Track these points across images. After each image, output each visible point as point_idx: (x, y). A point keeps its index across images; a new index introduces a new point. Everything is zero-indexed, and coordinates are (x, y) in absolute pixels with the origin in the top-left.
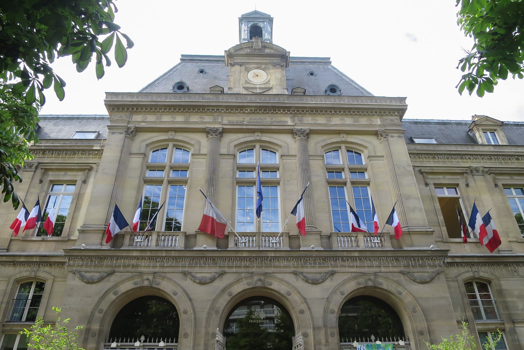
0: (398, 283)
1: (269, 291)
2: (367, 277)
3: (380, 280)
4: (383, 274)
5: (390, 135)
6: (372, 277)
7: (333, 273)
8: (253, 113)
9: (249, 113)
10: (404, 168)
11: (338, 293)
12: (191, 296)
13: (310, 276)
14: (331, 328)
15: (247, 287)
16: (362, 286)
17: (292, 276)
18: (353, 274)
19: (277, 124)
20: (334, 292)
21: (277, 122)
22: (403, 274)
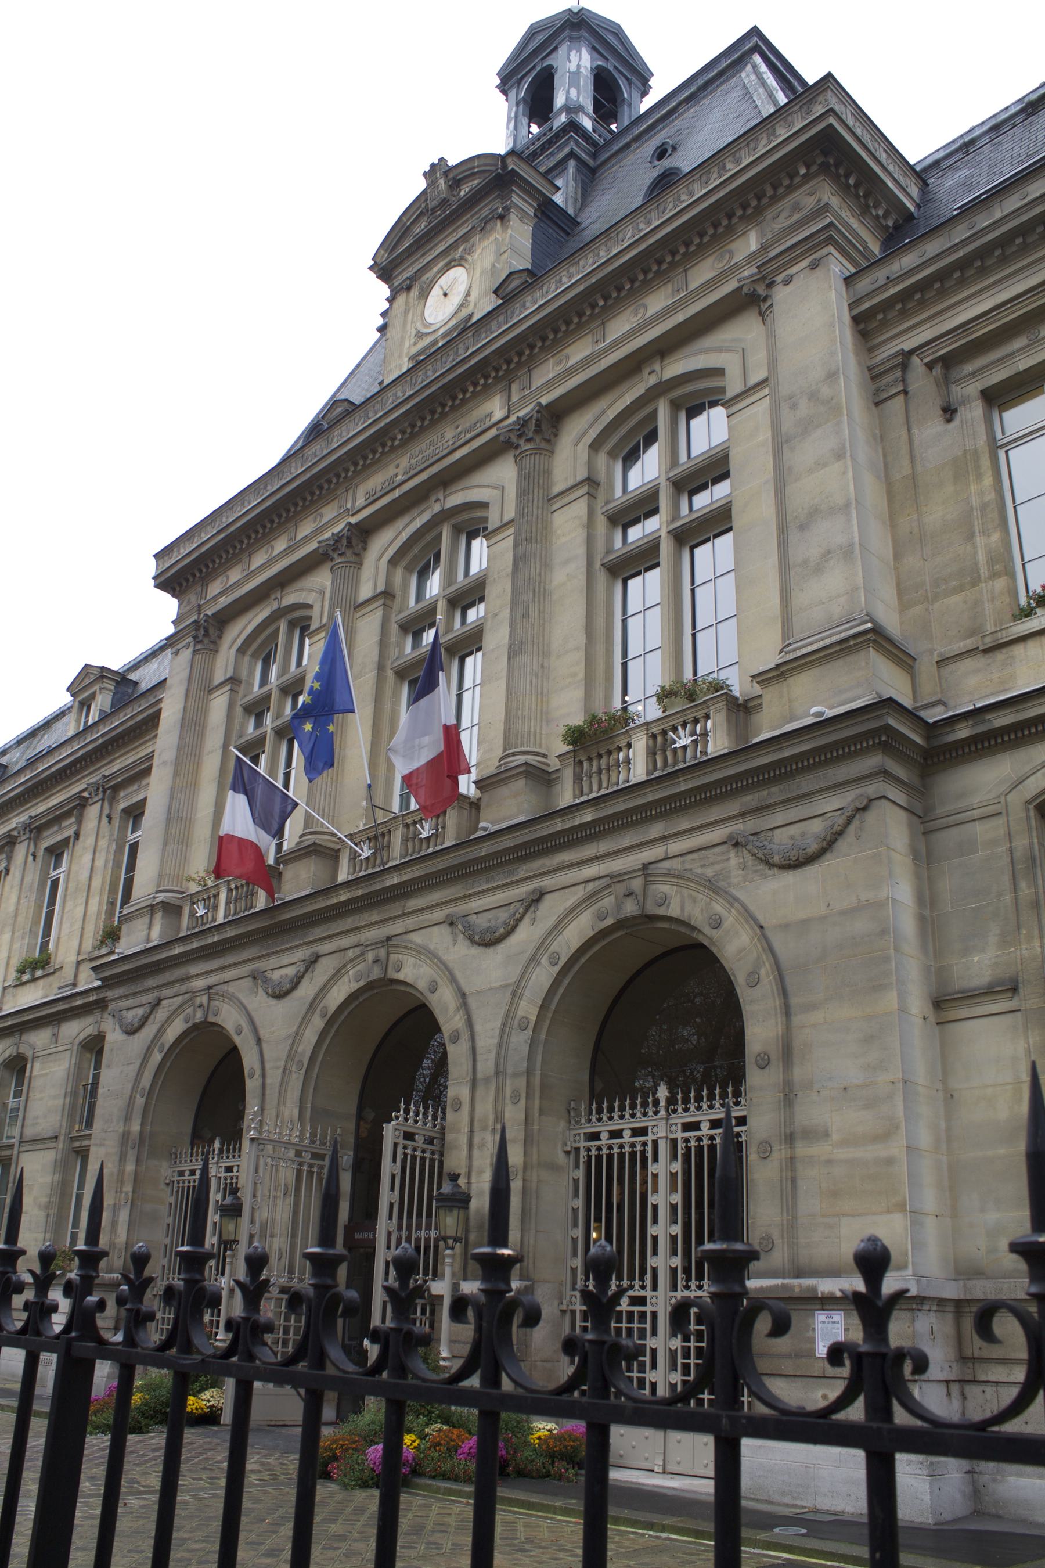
0: (713, 887)
1: (402, 988)
2: (620, 889)
3: (664, 888)
4: (675, 864)
5: (779, 279)
6: (637, 884)
7: (538, 897)
8: (413, 436)
9: (404, 443)
10: (813, 396)
11: (544, 961)
12: (262, 1033)
13: (482, 922)
14: (515, 1075)
15: (355, 986)
16: (609, 921)
17: (444, 930)
18: (591, 886)
19: (468, 436)
20: (534, 959)
21: (469, 430)
22: (736, 844)
